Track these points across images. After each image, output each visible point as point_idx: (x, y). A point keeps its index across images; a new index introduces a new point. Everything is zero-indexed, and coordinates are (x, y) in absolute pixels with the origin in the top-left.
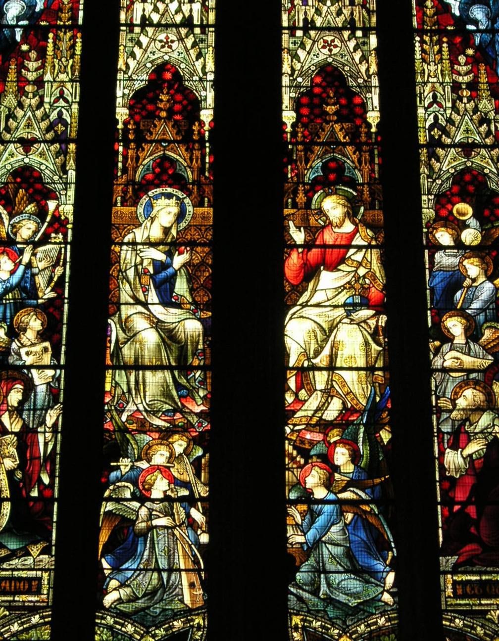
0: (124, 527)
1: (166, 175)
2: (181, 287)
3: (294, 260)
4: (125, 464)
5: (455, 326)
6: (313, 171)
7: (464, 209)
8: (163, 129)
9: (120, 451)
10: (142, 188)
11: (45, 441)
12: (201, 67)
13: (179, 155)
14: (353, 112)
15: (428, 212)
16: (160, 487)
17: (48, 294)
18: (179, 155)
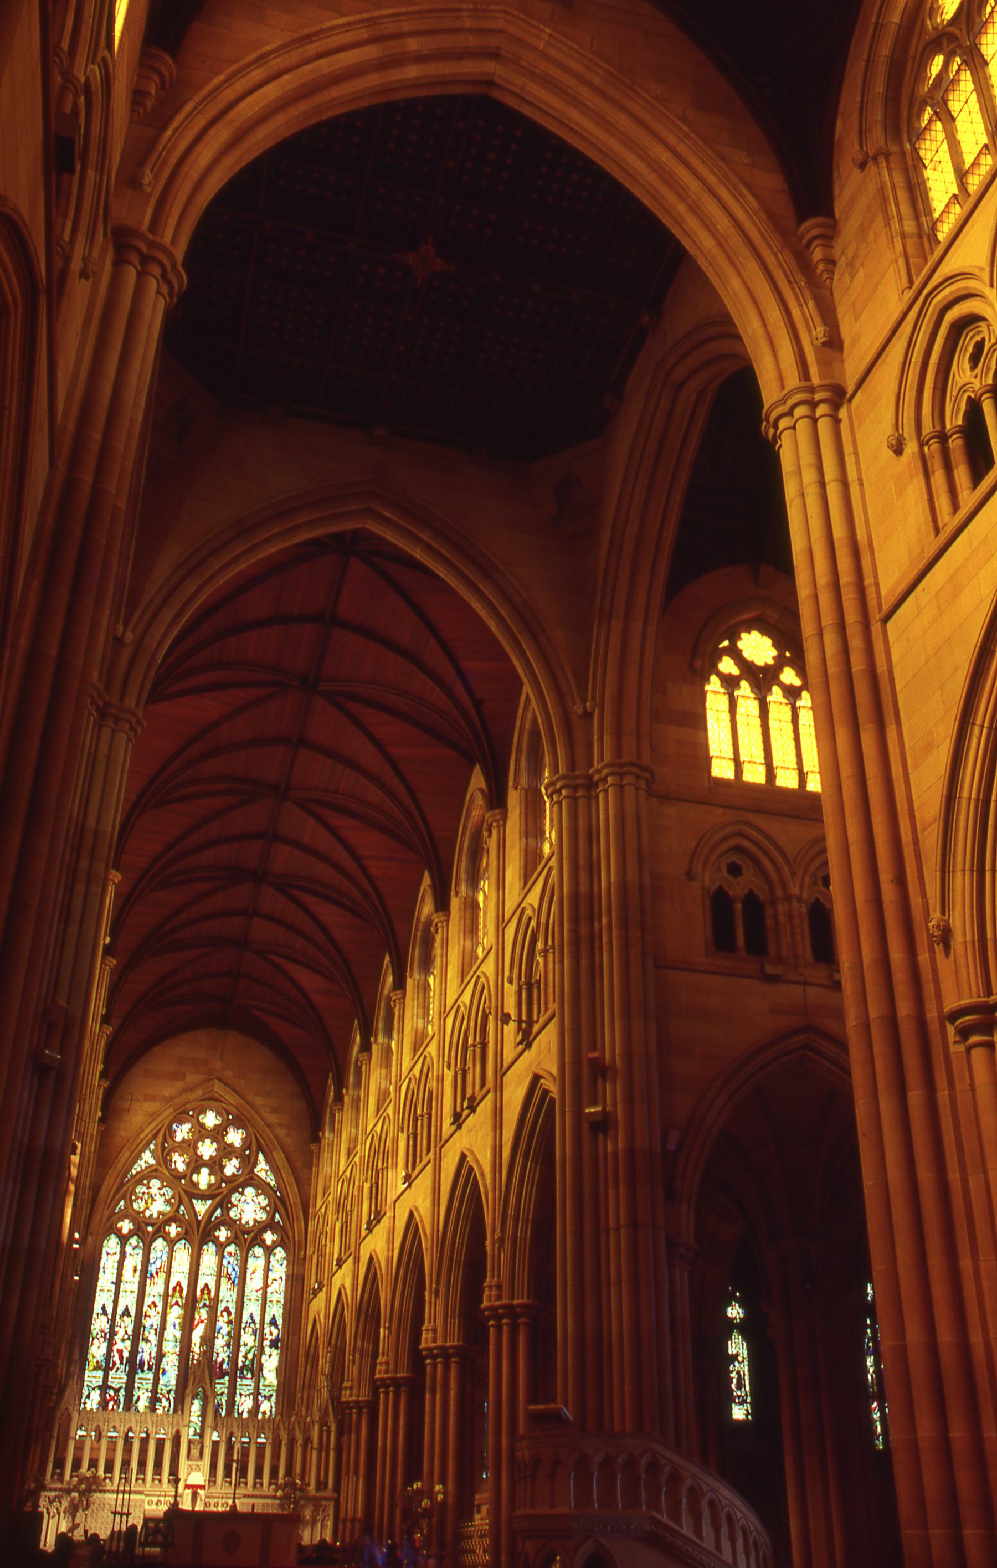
0: (164, 1370)
1: (177, 1303)
2: (177, 1327)
3: (196, 1322)
4: (164, 1359)
5: (220, 1336)
6: (201, 1304)
7: (225, 1314)
8: (177, 1294)
9: (164, 1356)
10: (172, 1306)
11: (154, 1355)
12: (185, 1285)
13: (179, 1300)
14: (209, 1293)
15: (219, 1314)
16: (171, 1363)
17: (155, 1327)
18: (179, 1300)
